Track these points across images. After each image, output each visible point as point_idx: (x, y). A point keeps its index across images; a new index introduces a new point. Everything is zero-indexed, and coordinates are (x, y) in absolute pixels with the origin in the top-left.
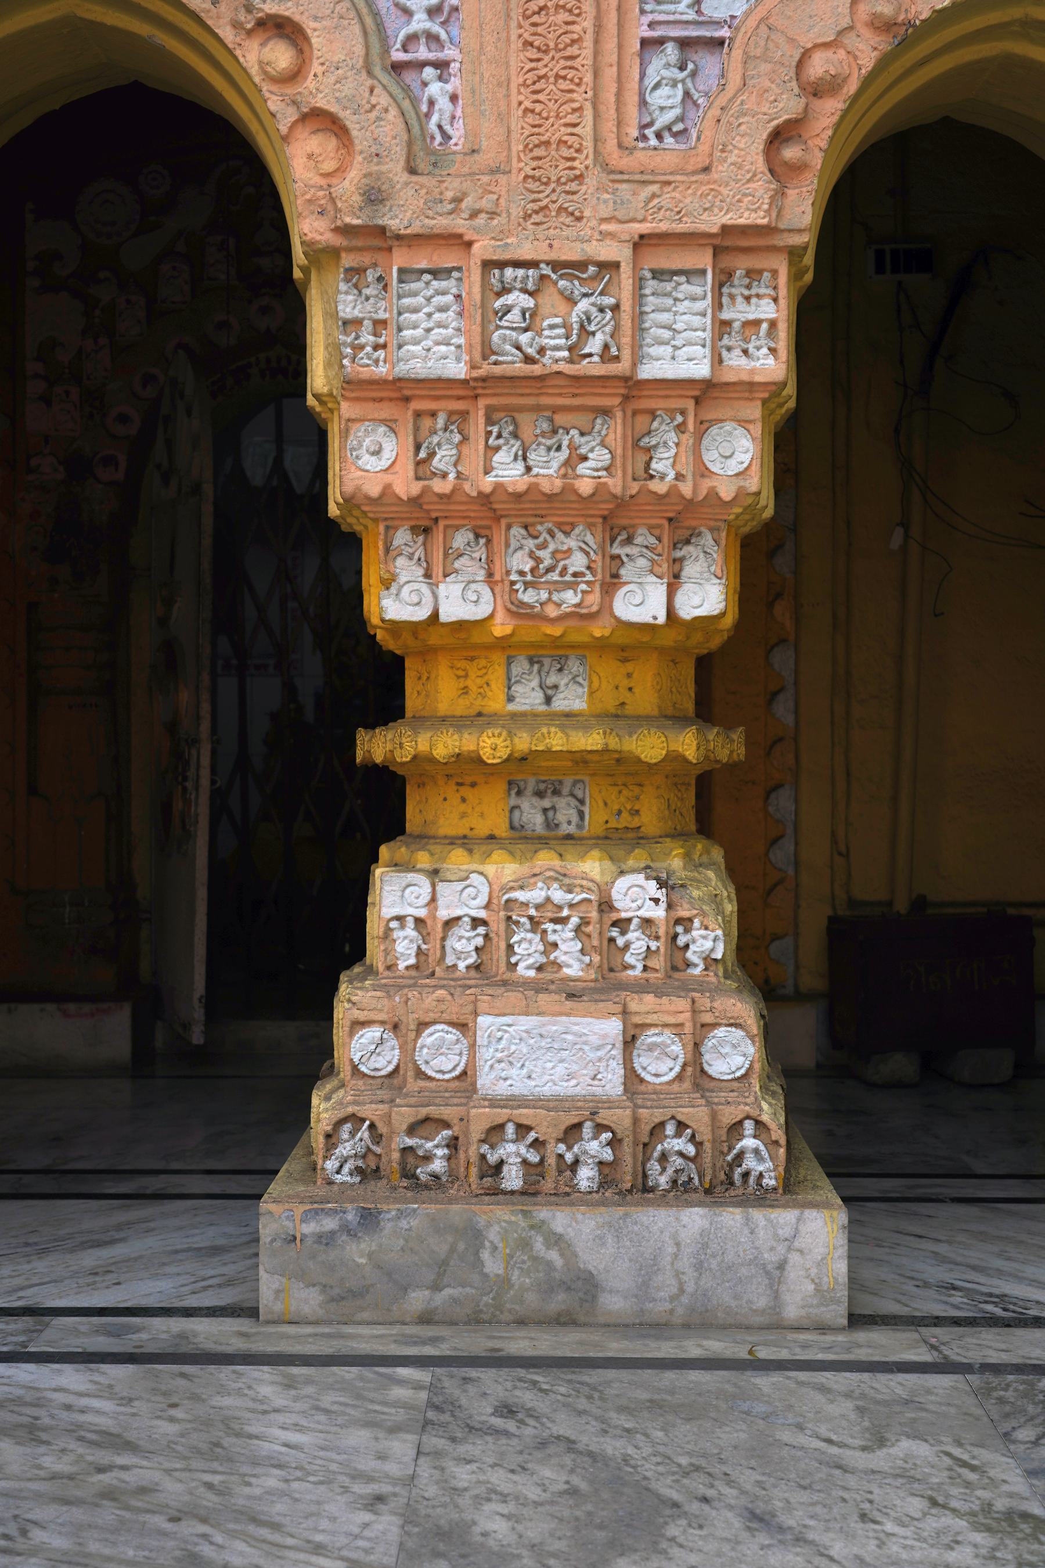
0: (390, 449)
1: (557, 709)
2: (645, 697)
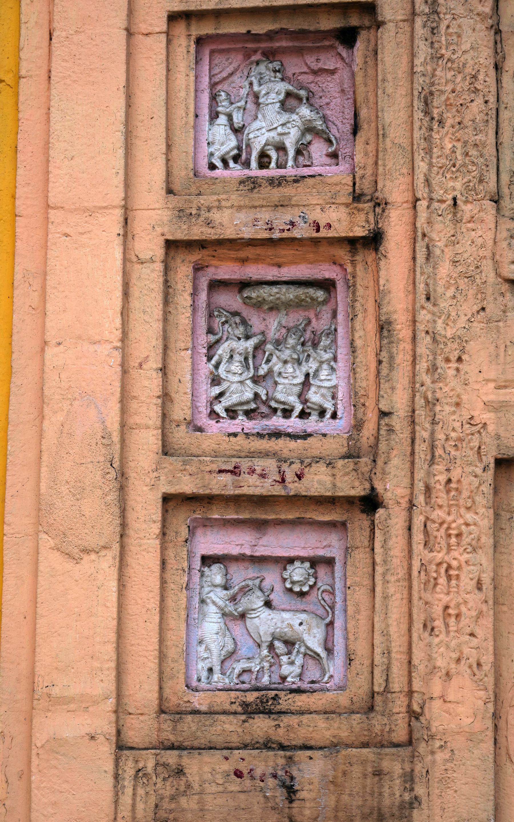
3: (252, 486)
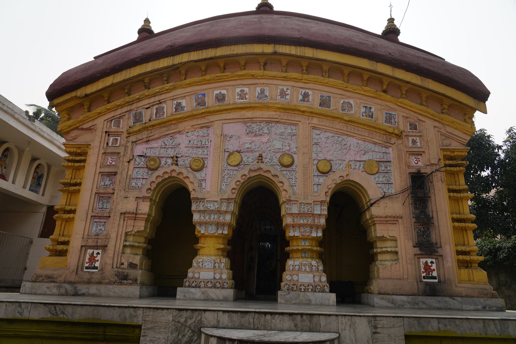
1: (306, 245)
2: (314, 244)
3: (99, 215)
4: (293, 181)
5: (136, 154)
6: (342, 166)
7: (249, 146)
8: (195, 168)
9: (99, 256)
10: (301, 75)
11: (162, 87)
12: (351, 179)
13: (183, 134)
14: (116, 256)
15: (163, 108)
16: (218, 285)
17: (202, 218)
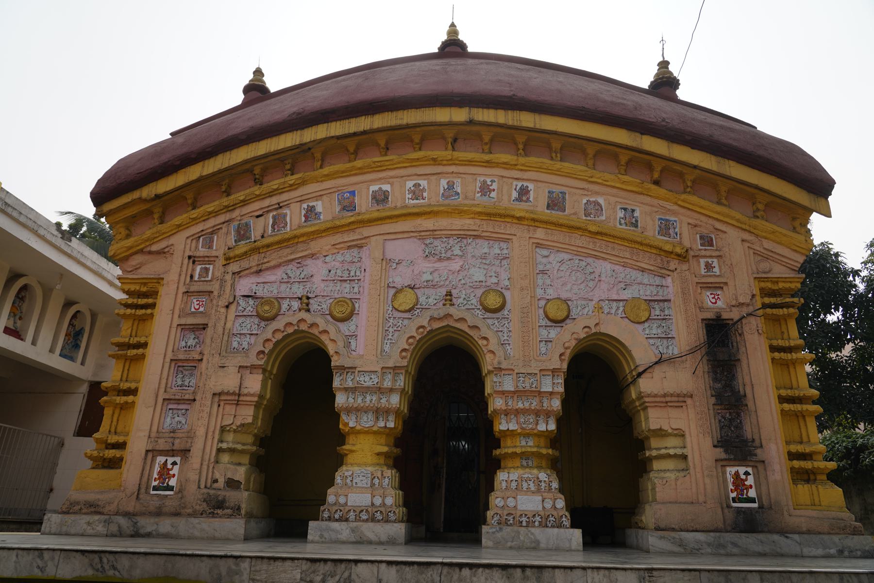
0: (501, 402)
1: (529, 445)
2: (542, 444)
3: (177, 397)
4: (505, 335)
5: (238, 293)
6: (587, 309)
7: (430, 278)
8: (339, 315)
9: (176, 468)
10: (515, 158)
11: (282, 180)
12: (603, 330)
13: (318, 258)
14: (205, 467)
15: (285, 215)
16: (379, 516)
17: (351, 400)
